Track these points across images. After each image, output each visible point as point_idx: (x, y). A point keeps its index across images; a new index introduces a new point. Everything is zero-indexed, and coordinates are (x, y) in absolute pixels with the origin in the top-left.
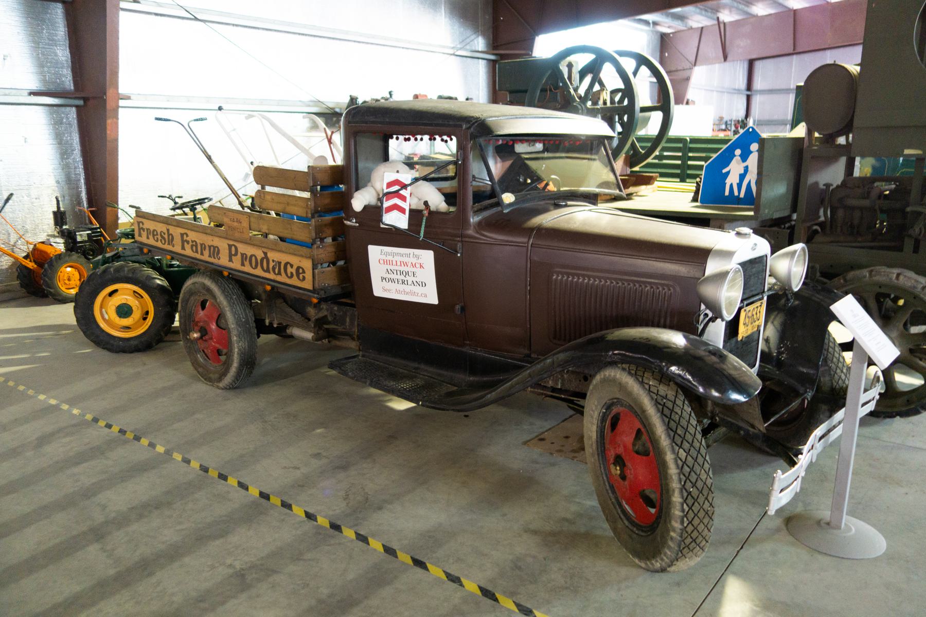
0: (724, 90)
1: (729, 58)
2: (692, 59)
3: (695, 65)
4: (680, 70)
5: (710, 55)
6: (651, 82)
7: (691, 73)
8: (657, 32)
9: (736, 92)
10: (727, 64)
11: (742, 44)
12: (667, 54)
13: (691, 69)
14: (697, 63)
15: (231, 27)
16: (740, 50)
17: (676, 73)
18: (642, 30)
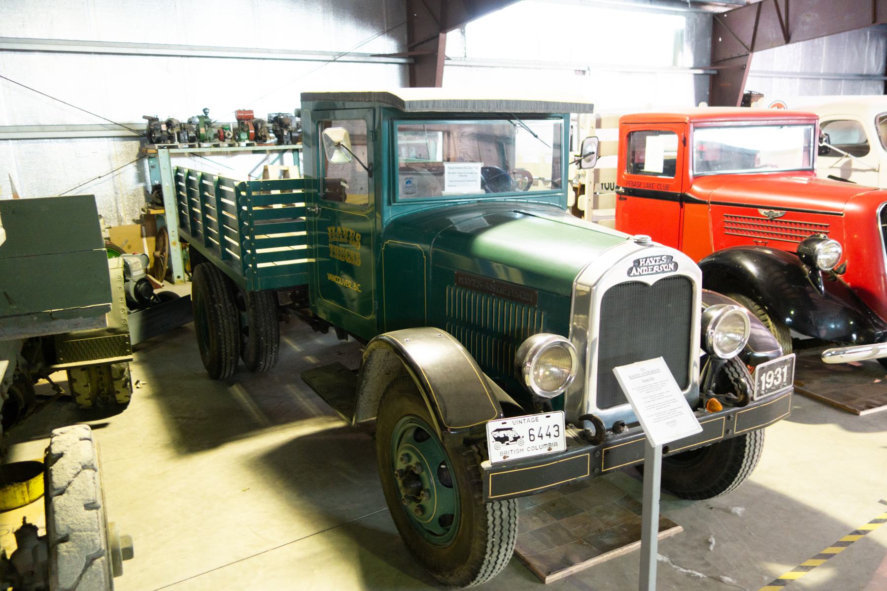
0: (841, 78)
1: (793, 38)
2: (748, 42)
3: (752, 50)
4: (736, 57)
5: (770, 36)
6: (695, 75)
7: (747, 60)
8: (706, 13)
9: (861, 78)
10: (790, 46)
11: (808, 20)
12: (720, 40)
13: (747, 55)
14: (755, 48)
15: (256, 60)
16: (806, 28)
17: (732, 61)
18: (676, 13)
